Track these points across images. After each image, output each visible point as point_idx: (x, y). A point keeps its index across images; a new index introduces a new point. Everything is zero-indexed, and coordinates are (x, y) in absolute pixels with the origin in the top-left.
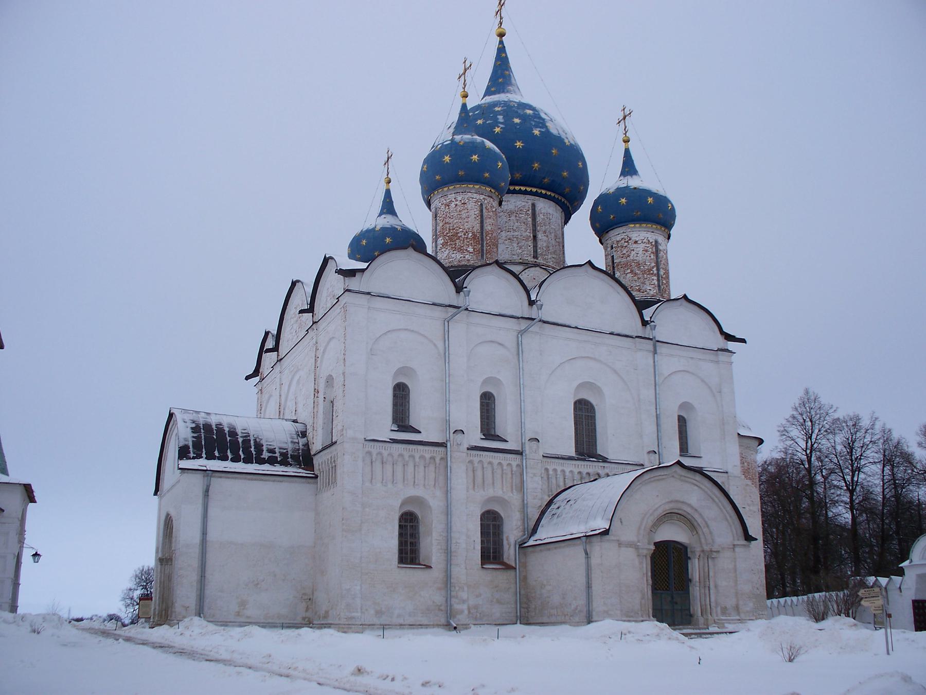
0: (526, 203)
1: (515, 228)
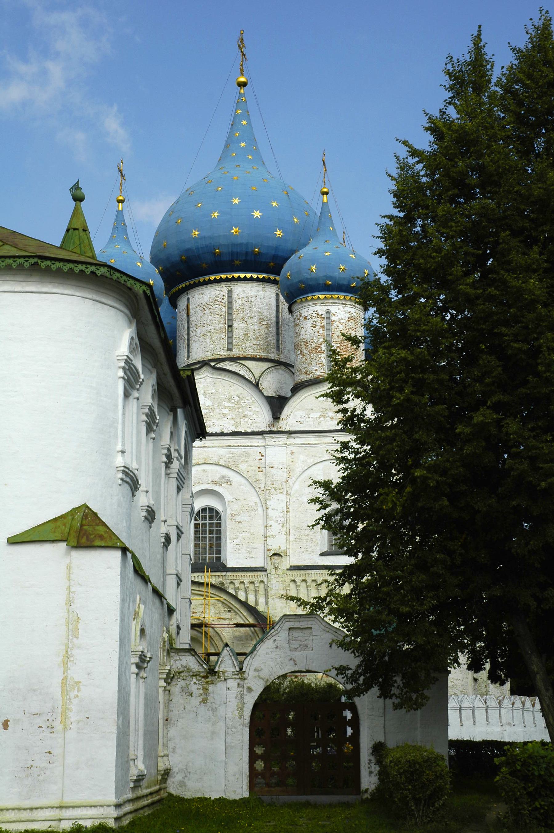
0: (220, 292)
1: (208, 322)
